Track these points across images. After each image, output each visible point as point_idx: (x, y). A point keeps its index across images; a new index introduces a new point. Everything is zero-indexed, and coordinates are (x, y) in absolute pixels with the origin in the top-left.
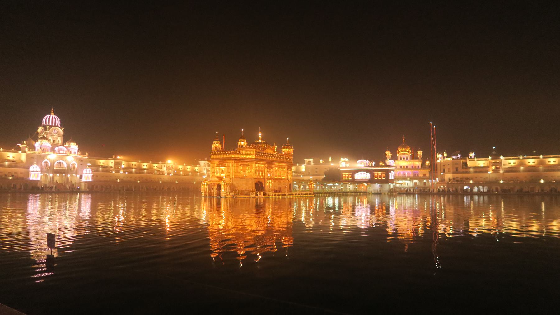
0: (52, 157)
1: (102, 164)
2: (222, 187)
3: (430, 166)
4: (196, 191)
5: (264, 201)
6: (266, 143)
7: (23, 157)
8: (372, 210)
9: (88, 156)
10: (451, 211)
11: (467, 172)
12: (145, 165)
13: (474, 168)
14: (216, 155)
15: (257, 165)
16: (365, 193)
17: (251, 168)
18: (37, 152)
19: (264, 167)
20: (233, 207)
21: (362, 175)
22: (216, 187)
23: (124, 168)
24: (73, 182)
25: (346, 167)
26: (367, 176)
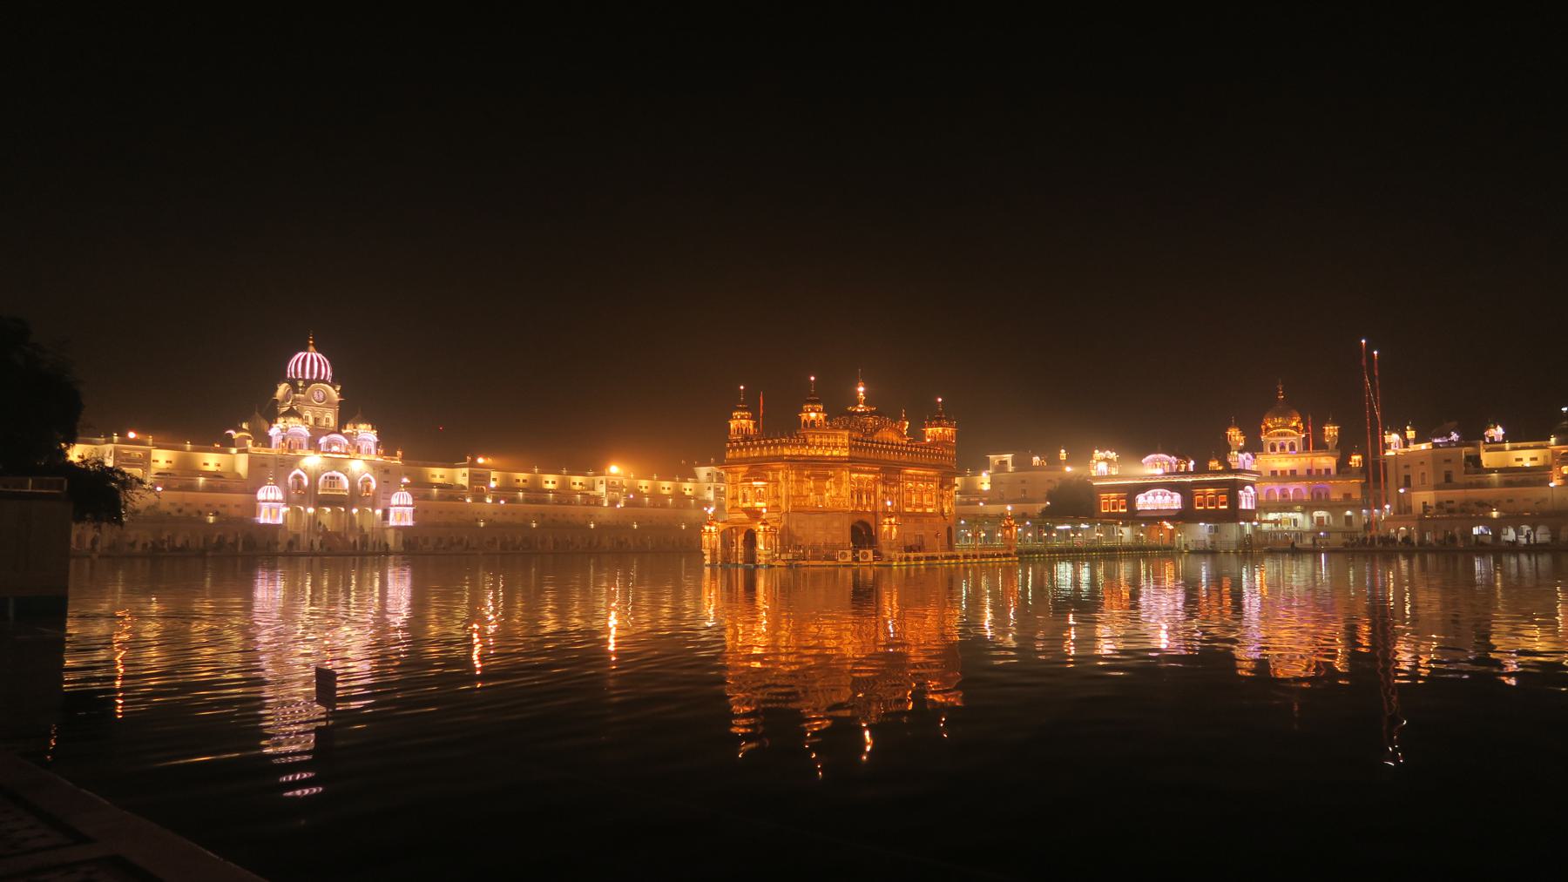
0: (312, 461)
1: (438, 480)
2: (760, 537)
3: (1363, 470)
5: (877, 576)
6: (878, 413)
7: (242, 464)
9: (402, 459)
10: (1432, 601)
11: (1480, 485)
12: (550, 482)
13: (1501, 470)
14: (741, 448)
15: (855, 476)
16: (1168, 552)
17: (839, 483)
18: (274, 450)
19: (875, 481)
20: (786, 593)
21: (1159, 498)
22: (741, 538)
23: (497, 489)
24: (367, 530)
25: (1110, 477)
26: (1174, 501)
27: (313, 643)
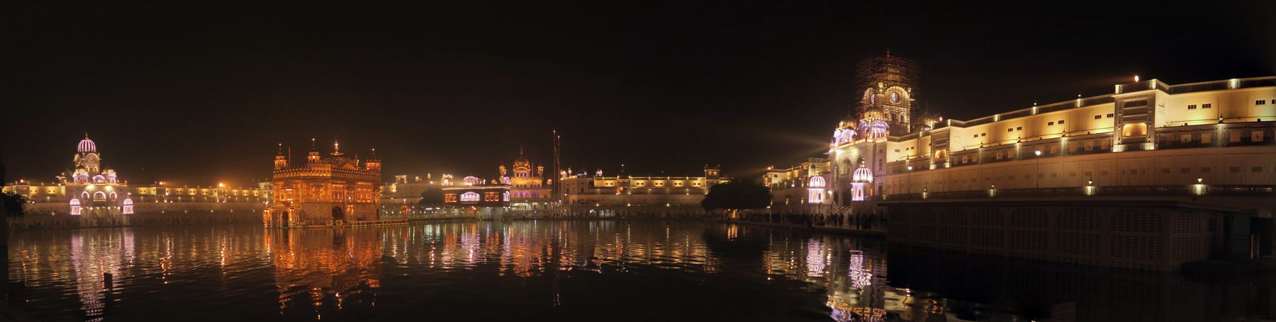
3: (552, 186)
4: (258, 220)
7: (63, 190)
8: (482, 241)
12: (192, 192)
16: (474, 219)
18: (75, 184)
26: (475, 197)
27: (96, 265)
